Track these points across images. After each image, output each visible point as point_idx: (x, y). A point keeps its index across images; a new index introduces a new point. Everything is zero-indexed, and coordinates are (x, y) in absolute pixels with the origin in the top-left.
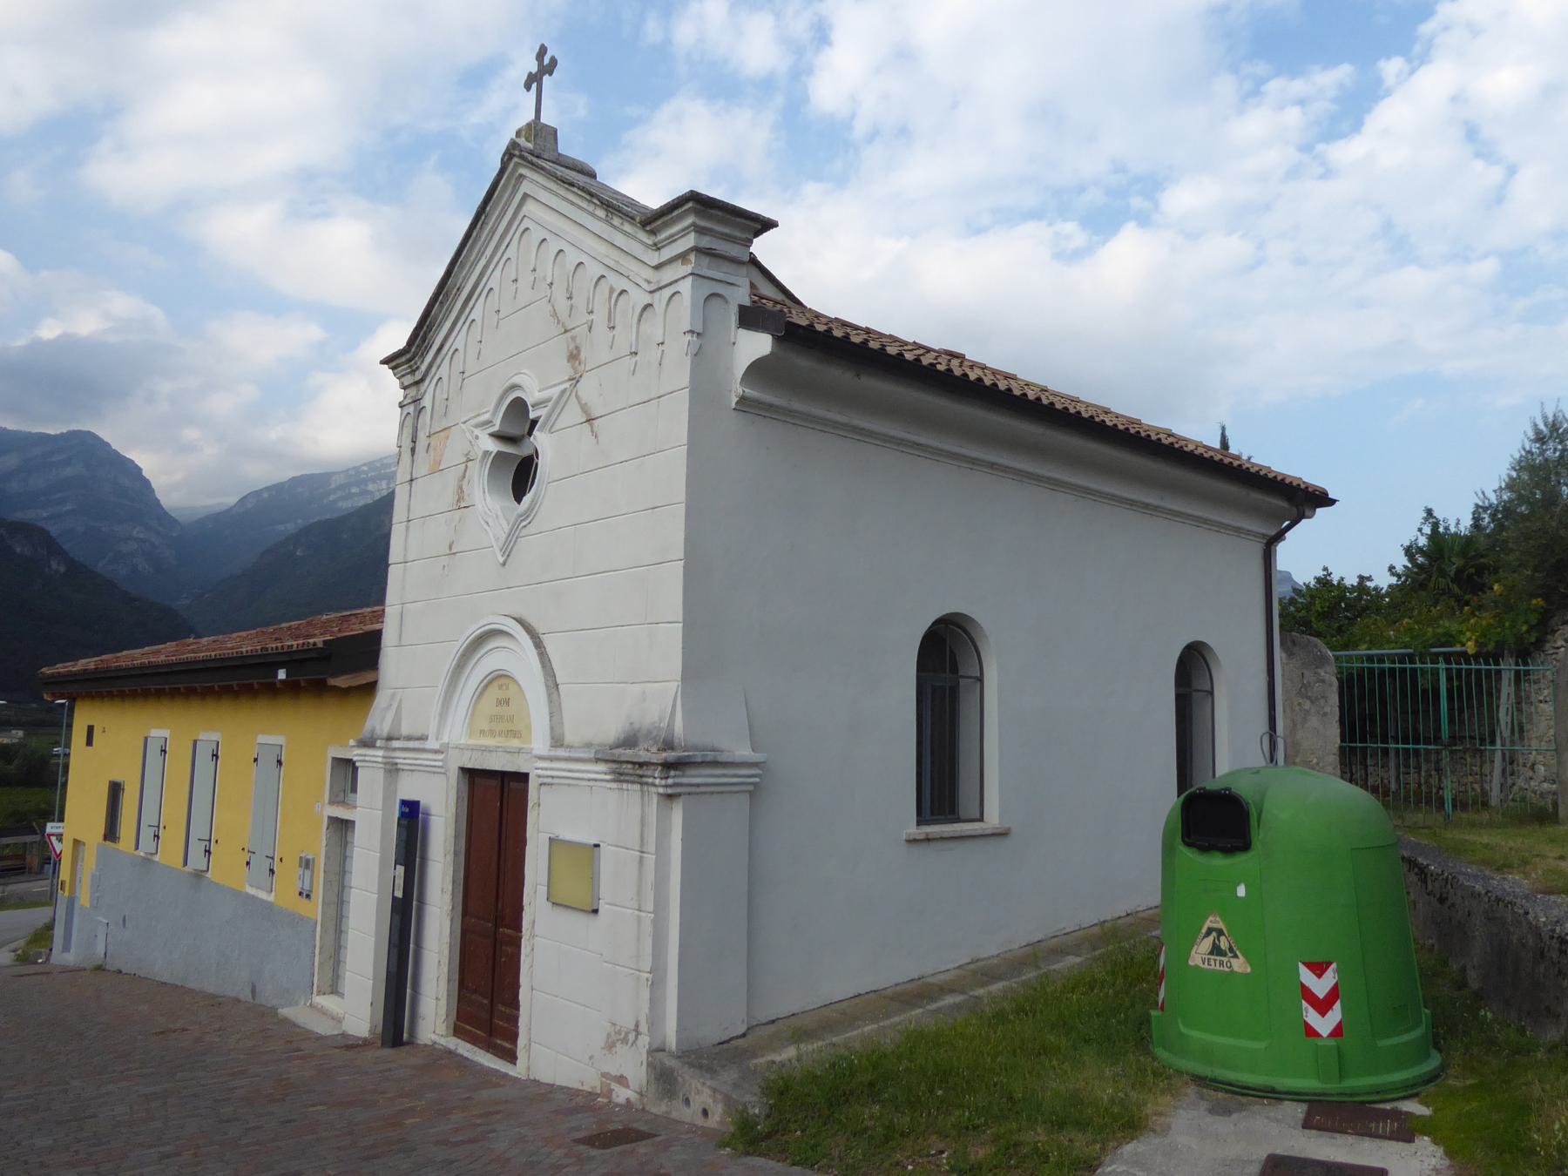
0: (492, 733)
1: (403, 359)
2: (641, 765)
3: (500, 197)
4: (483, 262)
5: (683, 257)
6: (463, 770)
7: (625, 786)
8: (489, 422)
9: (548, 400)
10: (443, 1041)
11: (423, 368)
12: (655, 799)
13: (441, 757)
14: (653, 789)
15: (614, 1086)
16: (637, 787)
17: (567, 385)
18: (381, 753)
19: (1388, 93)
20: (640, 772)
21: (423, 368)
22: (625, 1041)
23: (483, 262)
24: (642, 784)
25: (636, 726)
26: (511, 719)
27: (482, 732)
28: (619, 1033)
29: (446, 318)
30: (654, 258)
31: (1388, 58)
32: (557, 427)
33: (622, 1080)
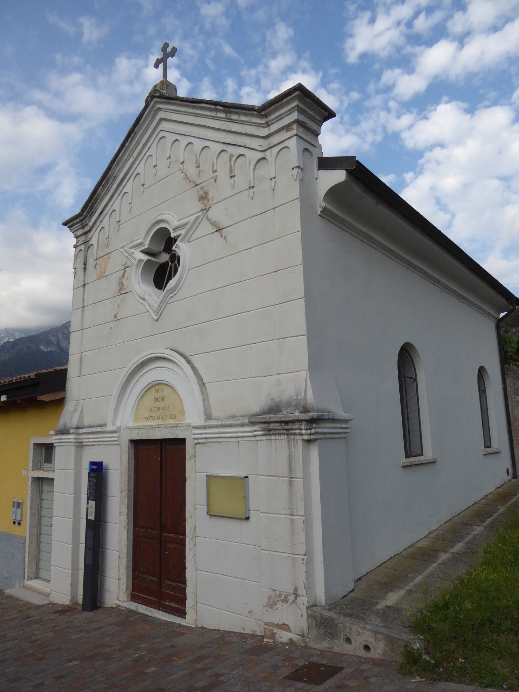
0: (152, 418)
1: (78, 220)
2: (287, 423)
3: (144, 123)
4: (131, 160)
5: (287, 128)
6: (134, 442)
7: (273, 437)
8: (141, 244)
9: (187, 224)
10: (126, 605)
11: (91, 224)
12: (300, 443)
13: (116, 435)
14: (301, 437)
15: (275, 630)
16: (286, 437)
17: (200, 214)
18: (73, 436)
19: (407, 185)
20: (286, 427)
21: (91, 224)
22: (285, 600)
23: (131, 160)
24: (288, 435)
25: (277, 400)
26: (167, 408)
27: (145, 418)
28: (279, 595)
29: (106, 194)
30: (265, 132)
31: (407, 173)
32: (193, 238)
33: (284, 627)
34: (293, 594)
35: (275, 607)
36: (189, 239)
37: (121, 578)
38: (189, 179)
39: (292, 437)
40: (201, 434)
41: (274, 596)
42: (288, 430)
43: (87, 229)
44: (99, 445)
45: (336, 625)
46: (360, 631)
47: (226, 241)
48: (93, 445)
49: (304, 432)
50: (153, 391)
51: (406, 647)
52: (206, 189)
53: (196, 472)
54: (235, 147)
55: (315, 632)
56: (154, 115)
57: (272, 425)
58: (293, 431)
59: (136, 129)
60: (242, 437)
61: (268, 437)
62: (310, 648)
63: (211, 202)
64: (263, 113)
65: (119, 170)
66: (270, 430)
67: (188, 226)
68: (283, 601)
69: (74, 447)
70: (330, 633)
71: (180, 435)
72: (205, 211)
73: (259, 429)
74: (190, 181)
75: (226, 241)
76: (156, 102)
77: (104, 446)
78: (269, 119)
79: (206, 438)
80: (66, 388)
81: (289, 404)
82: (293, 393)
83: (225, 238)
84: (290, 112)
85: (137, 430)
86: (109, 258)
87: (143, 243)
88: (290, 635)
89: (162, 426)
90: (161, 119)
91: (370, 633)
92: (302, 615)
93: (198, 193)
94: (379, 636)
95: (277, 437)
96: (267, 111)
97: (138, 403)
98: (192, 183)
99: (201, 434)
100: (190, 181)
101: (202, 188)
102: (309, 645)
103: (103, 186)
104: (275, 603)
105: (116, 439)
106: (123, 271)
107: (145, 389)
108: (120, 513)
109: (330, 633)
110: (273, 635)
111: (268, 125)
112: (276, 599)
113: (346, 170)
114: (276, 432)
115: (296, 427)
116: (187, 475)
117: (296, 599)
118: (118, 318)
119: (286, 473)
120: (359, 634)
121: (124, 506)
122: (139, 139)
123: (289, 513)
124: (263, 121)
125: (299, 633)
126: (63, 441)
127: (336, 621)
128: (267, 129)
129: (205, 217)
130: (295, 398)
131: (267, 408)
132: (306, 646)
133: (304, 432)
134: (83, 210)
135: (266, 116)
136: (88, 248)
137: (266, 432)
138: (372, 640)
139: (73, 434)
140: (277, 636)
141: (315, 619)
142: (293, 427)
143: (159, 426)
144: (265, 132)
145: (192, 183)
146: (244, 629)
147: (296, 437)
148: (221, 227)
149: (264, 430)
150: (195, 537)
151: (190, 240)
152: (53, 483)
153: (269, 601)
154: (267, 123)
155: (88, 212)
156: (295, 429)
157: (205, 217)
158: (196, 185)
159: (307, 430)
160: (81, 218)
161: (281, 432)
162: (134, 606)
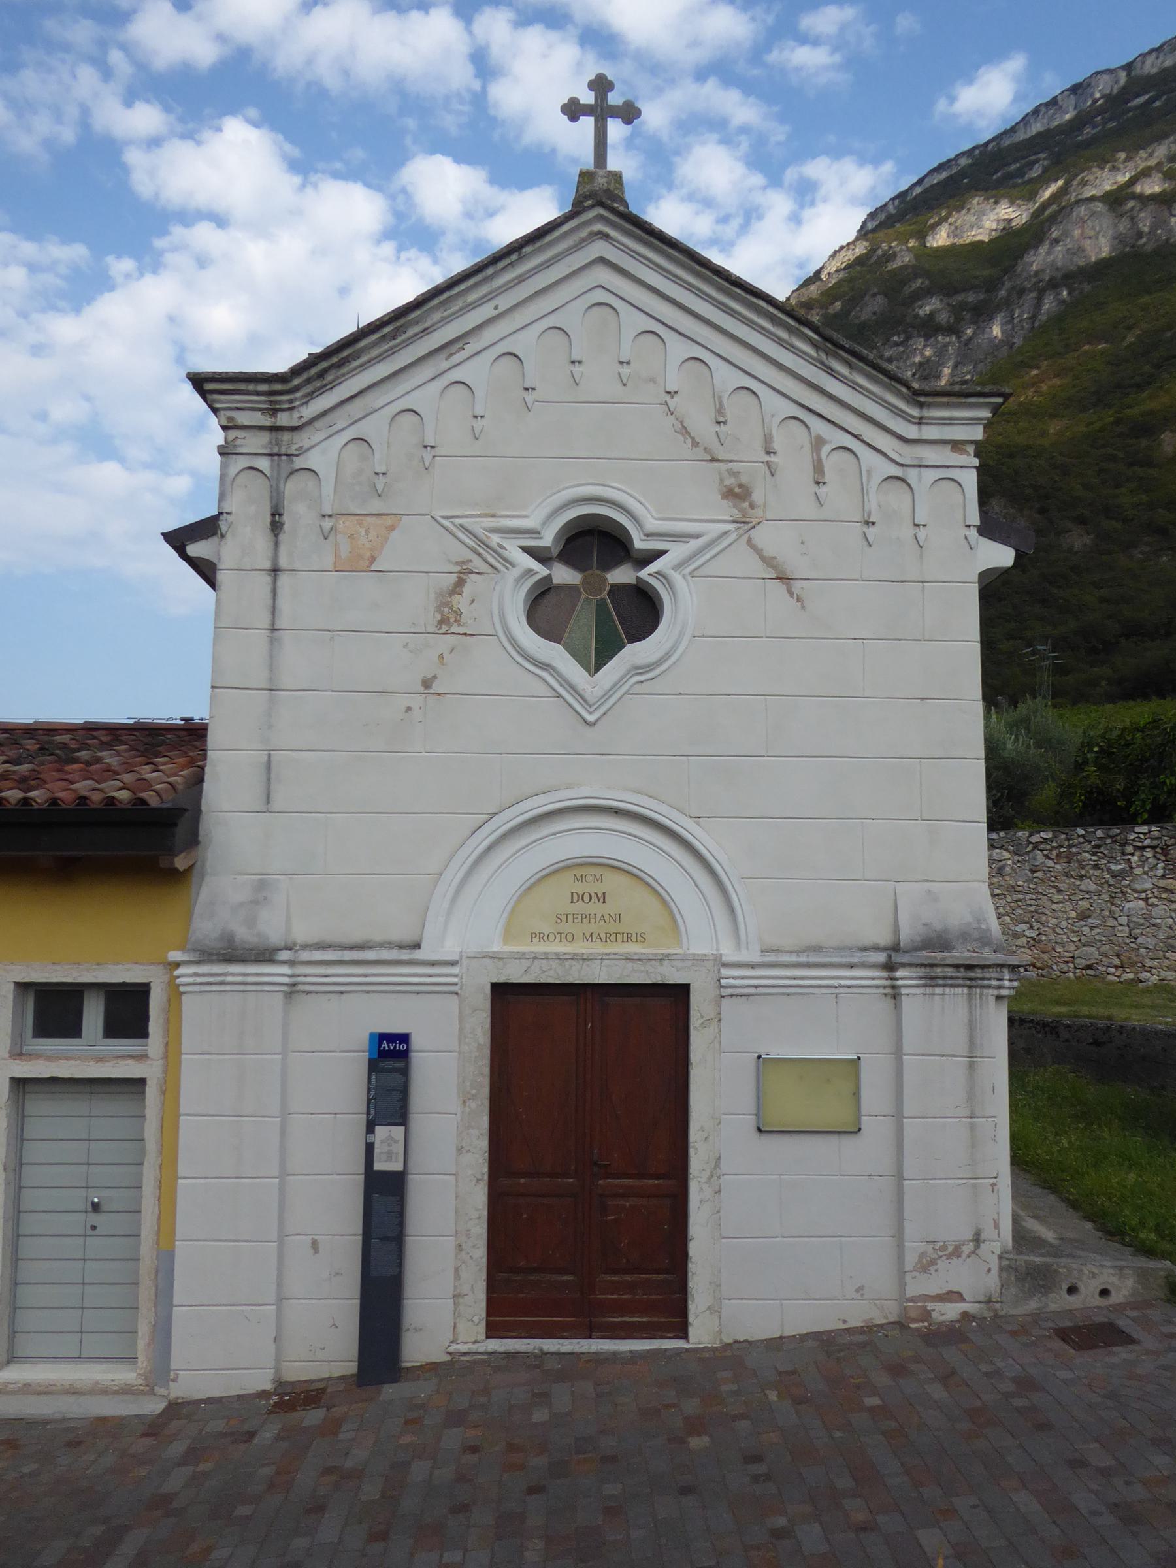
0: (563, 937)
1: (264, 387)
2: (969, 967)
3: (550, 244)
4: (486, 311)
5: (956, 445)
6: (501, 991)
7: (938, 990)
8: (534, 533)
9: (697, 536)
10: (481, 1348)
11: (308, 412)
12: (992, 1000)
13: (455, 970)
14: (991, 991)
15: (930, 1306)
16: (965, 990)
17: (731, 527)
18: (285, 970)
19: (112, 288)
20: (972, 975)
21: (308, 412)
22: (956, 1253)
23: (486, 311)
24: (970, 987)
25: (938, 927)
26: (618, 919)
27: (541, 937)
28: (944, 1248)
29: (380, 358)
30: (911, 432)
31: (119, 257)
32: (705, 571)
33: (953, 1296)
34: (972, 1241)
35: (932, 1269)
36: (695, 570)
37: (465, 1289)
38: (693, 439)
39: (978, 991)
40: (742, 978)
41: (931, 1251)
42: (970, 979)
43: (283, 419)
44: (368, 992)
45: (1055, 1271)
46: (1096, 1271)
47: (803, 607)
48: (342, 993)
49: (1007, 983)
50: (568, 877)
51: (1166, 1277)
52: (744, 479)
53: (721, 1052)
54: (829, 425)
55: (1013, 1290)
56: (583, 240)
57: (939, 970)
58: (986, 982)
59: (528, 249)
60: (849, 987)
61: (928, 990)
62: (1002, 1316)
63: (758, 512)
64: (922, 399)
65: (443, 319)
66: (932, 978)
67: (694, 544)
68: (949, 1256)
69: (281, 996)
70: (1043, 1286)
71: (672, 975)
72: (747, 527)
73: (915, 975)
74: (695, 444)
75: (803, 607)
76: (600, 218)
77: (394, 996)
78: (927, 413)
79: (756, 987)
80: (200, 838)
81: (965, 936)
82: (969, 918)
83: (798, 600)
84: (973, 421)
85: (528, 963)
86: (392, 528)
87: (539, 533)
88: (961, 1307)
89: (617, 957)
90: (602, 260)
91: (1111, 1271)
92: (989, 1270)
93: (721, 480)
94: (1126, 1271)
95: (947, 990)
96: (929, 399)
97: (519, 900)
98: (700, 450)
99: (742, 978)
100: (695, 444)
101: (734, 474)
102: (1000, 1313)
103: (383, 336)
104: (933, 1262)
105: (455, 980)
106: (453, 578)
107: (547, 871)
108: (460, 1149)
109: (1043, 1286)
110: (926, 1315)
111: (920, 422)
112: (935, 1256)
113: (1016, 550)
114: (949, 982)
115: (993, 975)
116: (693, 1057)
117: (977, 1247)
118: (436, 687)
119: (962, 1048)
120: (1094, 1275)
121: (475, 1132)
122: (525, 273)
123: (968, 1114)
124: (915, 412)
125: (982, 1298)
126: (229, 979)
127: (1055, 1267)
128: (916, 427)
129: (745, 538)
130: (975, 926)
131: (919, 939)
132: (996, 1316)
133: (1007, 983)
134: (296, 371)
135: (921, 405)
136: (291, 473)
137: (929, 982)
138: (1115, 1279)
139: (284, 962)
140: (934, 1315)
141: (1016, 1270)
142: (987, 975)
143: (604, 956)
144: (911, 432)
145: (700, 450)
146: (845, 1322)
147: (985, 991)
148: (789, 574)
149: (920, 978)
150: (719, 1177)
151: (696, 573)
152: (144, 1092)
153: (920, 1261)
154: (921, 418)
155: (309, 381)
156: (990, 979)
157: (746, 536)
158: (714, 460)
159: (1010, 980)
160: (278, 387)
161: (961, 982)
162: (495, 1345)
